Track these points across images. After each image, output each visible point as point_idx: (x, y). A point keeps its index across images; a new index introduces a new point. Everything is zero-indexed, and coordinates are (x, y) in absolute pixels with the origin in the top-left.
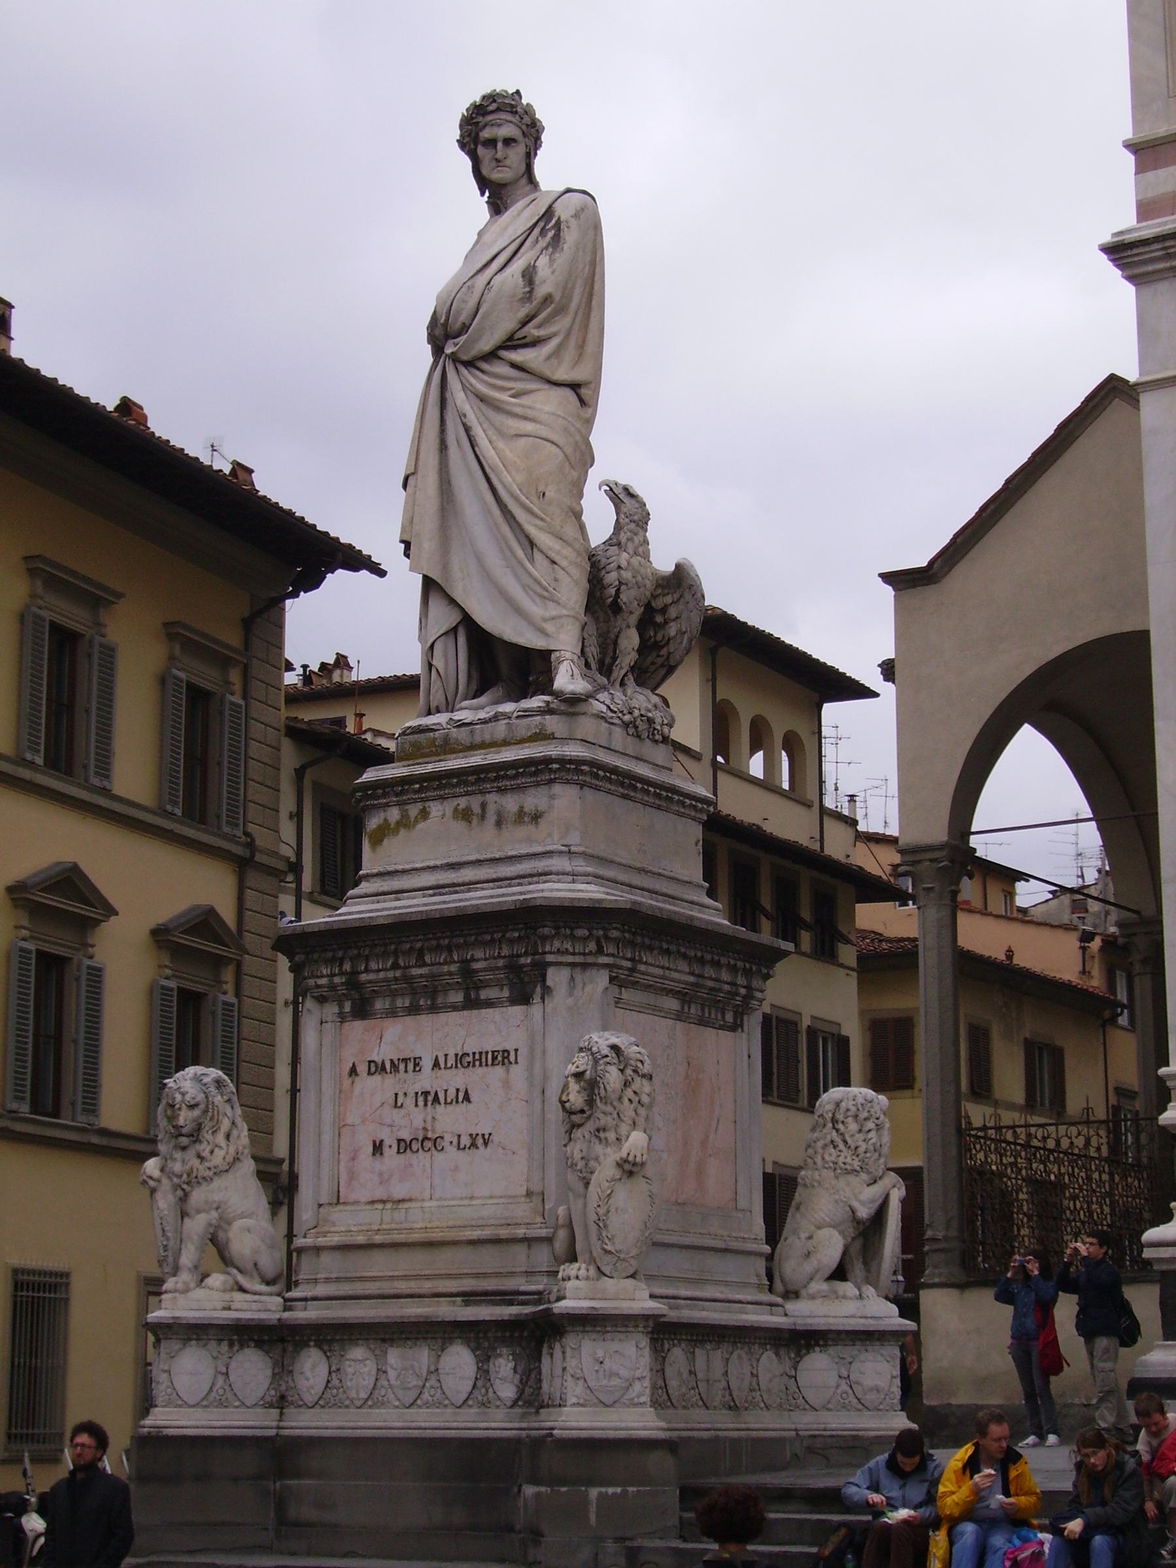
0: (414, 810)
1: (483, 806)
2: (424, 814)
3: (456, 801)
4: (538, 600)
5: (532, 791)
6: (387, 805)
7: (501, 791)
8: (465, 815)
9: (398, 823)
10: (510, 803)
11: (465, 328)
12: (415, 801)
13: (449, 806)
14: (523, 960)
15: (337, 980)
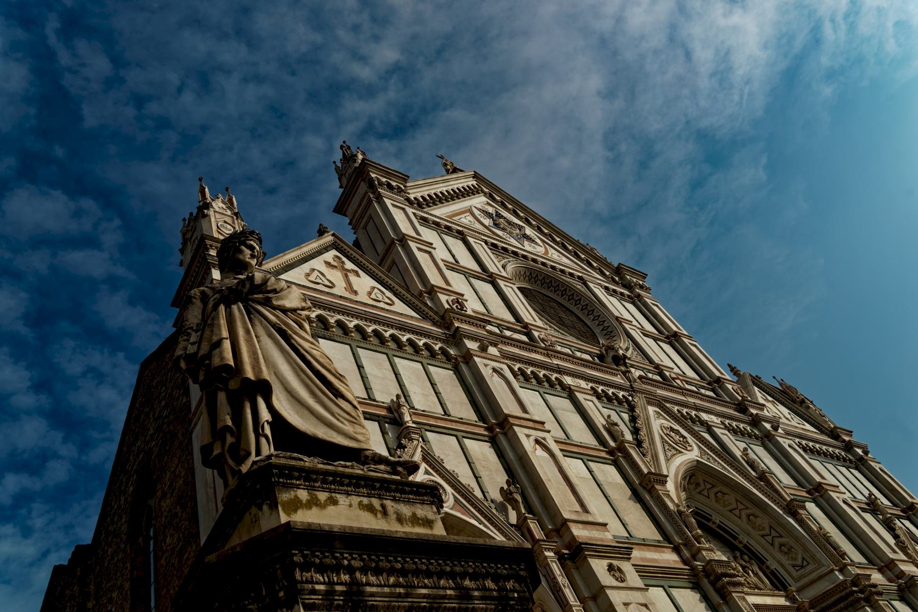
0: (322, 496)
1: (383, 506)
2: (335, 502)
3: (362, 498)
4: (346, 422)
5: (419, 505)
6: (298, 487)
7: (394, 500)
8: (370, 509)
9: (308, 501)
10: (406, 510)
11: (275, 291)
12: (324, 490)
13: (355, 500)
14: (511, 595)
15: (339, 588)
